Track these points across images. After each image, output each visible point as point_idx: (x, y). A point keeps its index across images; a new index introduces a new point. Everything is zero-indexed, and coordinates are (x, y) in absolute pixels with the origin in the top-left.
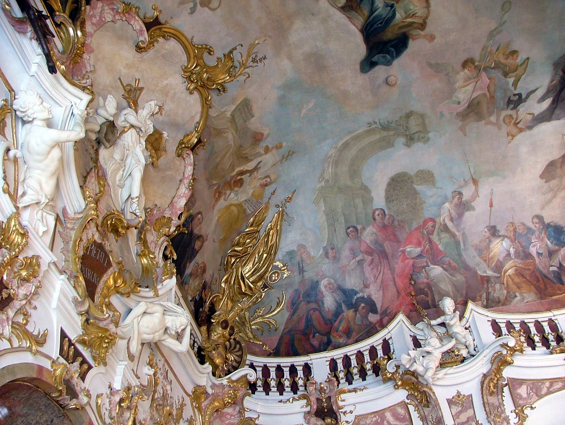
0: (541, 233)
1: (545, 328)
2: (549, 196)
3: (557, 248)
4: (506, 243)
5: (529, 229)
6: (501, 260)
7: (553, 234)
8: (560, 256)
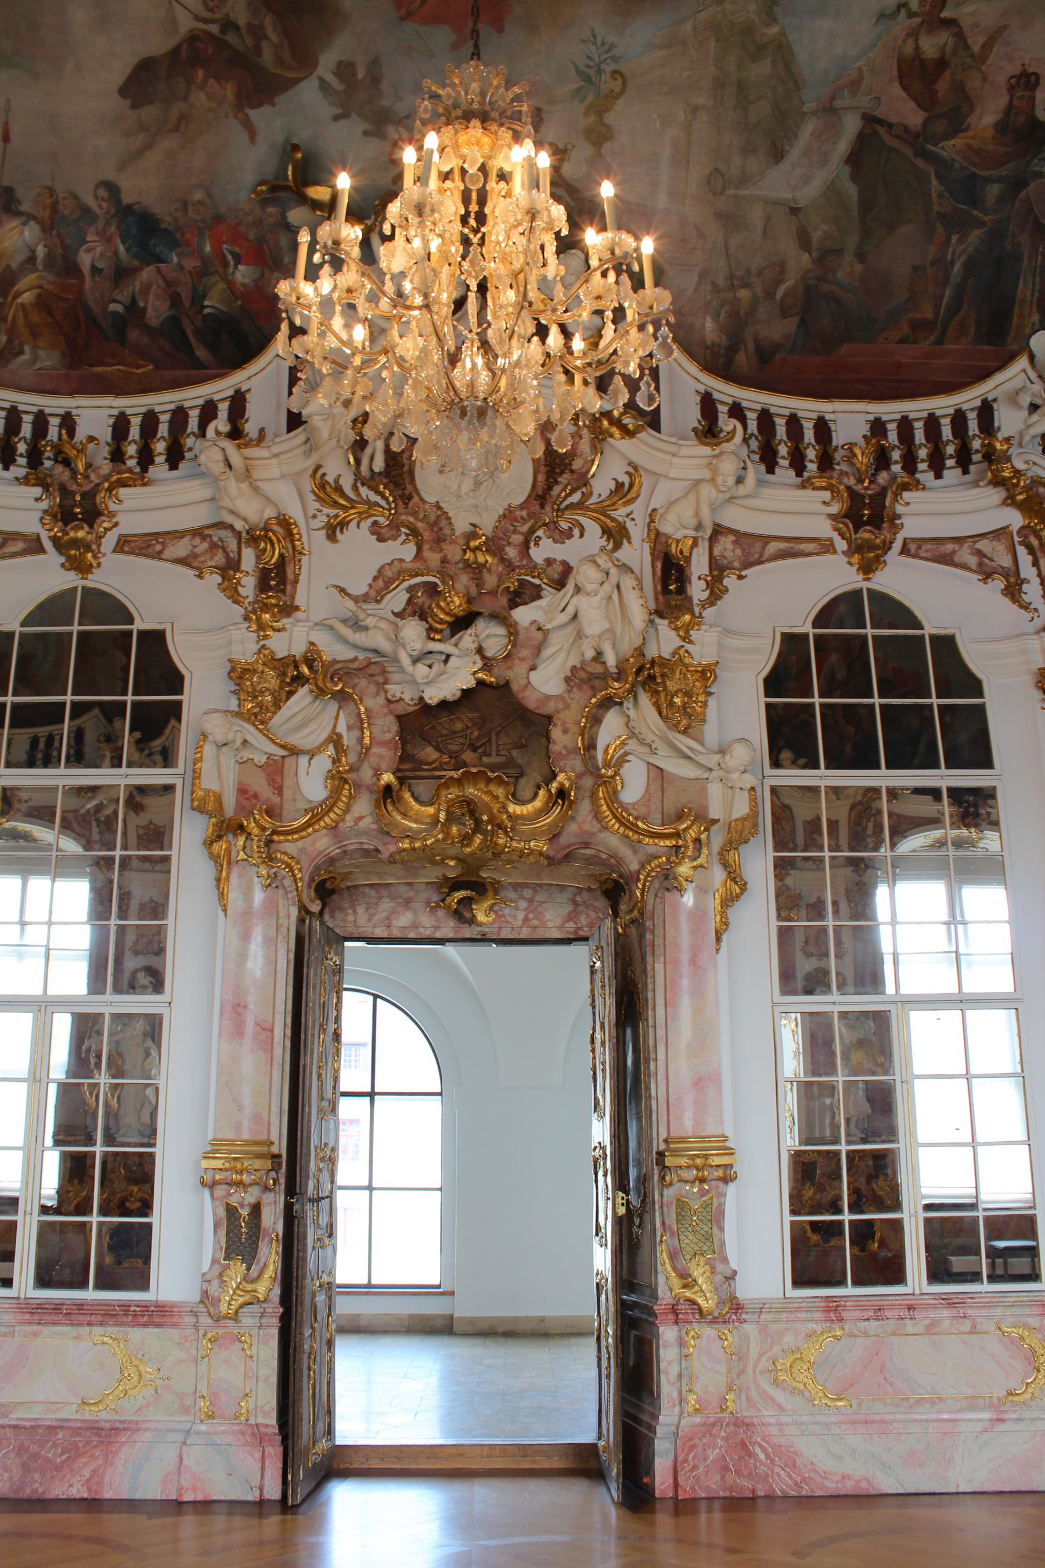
0: (108, 223)
1: (51, 428)
2: (138, 141)
3: (136, 263)
4: (30, 233)
5: (86, 210)
6: (14, 266)
7: (134, 231)
8: (137, 284)
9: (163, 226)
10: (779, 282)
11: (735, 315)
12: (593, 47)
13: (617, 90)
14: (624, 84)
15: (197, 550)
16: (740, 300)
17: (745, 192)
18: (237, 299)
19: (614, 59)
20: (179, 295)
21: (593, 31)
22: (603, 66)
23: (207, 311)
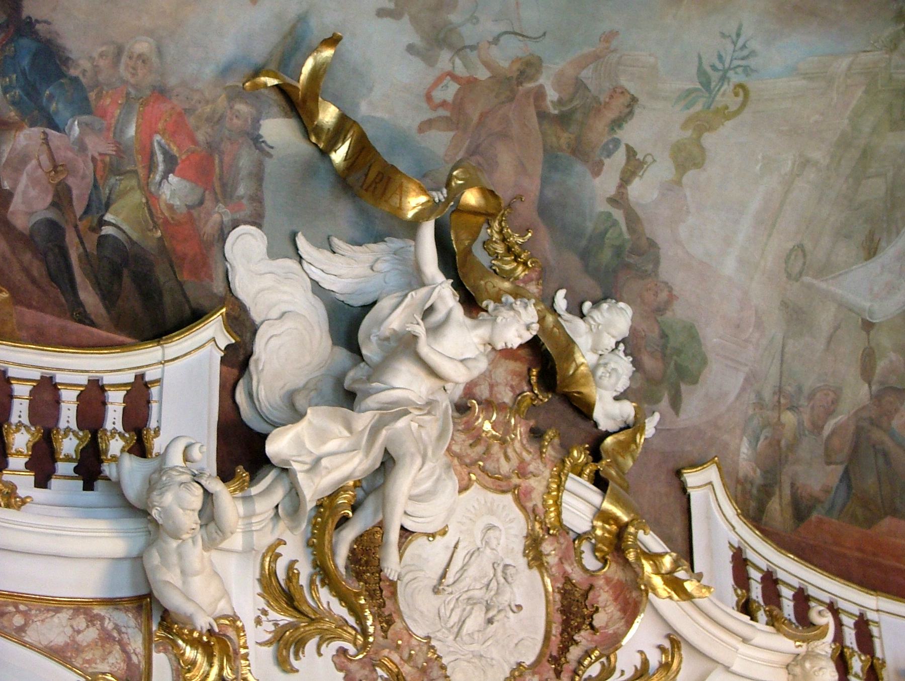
9: (73, 72)
10: (830, 413)
11: (774, 443)
12: (730, 47)
13: (733, 108)
14: (744, 105)
15: (79, 638)
16: (783, 425)
17: (823, 285)
18: (156, 226)
19: (747, 70)
20: (69, 190)
21: (740, 28)
22: (731, 74)
23: (107, 230)
